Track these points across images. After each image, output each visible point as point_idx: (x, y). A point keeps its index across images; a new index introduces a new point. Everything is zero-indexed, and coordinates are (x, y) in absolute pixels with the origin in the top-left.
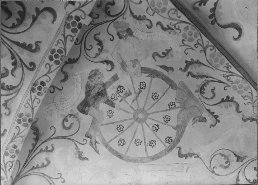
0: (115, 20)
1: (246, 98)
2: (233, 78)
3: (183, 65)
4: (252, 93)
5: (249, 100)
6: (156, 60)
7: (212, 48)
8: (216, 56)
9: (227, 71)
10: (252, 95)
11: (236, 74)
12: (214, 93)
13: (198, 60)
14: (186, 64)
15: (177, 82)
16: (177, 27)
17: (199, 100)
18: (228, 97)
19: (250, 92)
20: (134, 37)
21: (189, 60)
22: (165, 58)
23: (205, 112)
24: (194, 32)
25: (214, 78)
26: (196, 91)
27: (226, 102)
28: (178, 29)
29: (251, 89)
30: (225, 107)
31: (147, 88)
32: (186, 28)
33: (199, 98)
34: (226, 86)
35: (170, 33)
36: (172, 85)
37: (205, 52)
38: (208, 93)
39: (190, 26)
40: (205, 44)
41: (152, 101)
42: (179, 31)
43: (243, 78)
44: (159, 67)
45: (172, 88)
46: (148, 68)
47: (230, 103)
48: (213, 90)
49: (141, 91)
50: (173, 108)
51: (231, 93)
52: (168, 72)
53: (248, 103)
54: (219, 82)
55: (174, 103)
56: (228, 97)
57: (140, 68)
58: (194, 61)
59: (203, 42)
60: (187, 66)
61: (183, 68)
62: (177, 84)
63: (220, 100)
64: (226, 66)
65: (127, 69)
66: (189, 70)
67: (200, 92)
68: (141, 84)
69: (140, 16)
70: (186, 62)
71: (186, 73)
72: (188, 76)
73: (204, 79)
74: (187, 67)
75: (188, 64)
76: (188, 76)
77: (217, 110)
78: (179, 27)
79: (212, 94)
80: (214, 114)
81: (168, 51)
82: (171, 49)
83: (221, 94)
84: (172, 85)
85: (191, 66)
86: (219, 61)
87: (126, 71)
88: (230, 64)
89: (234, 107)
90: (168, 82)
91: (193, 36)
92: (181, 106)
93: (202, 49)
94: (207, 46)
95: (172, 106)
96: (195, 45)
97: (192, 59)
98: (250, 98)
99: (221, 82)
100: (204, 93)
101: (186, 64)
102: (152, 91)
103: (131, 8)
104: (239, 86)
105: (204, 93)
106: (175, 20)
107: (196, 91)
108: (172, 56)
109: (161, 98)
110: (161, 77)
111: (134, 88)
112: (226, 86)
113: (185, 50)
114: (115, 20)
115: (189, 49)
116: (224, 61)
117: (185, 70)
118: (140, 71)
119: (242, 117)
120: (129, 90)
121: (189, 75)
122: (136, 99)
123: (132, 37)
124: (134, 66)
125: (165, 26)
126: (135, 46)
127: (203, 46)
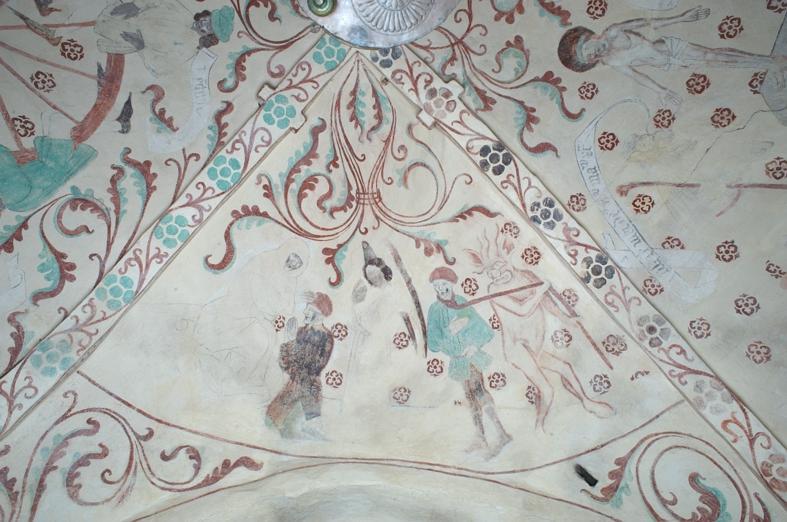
0: (239, 13)
1: (88, 309)
2: (133, 273)
3: (138, 156)
4: (104, 319)
5: (83, 318)
6: (144, 92)
7: (197, 218)
8: (180, 229)
9: (150, 257)
10: (99, 321)
11: (145, 275)
12: (76, 233)
13: (155, 188)
14: (142, 162)
15: (94, 141)
16: (238, 145)
17: (53, 199)
18: (72, 267)
19: (105, 313)
20: (198, 48)
21: (152, 170)
22: (151, 115)
23: (17, 217)
24: (229, 179)
25: (116, 227)
26: (74, 189)
27: (56, 265)
28: (233, 148)
29: (114, 314)
30: (43, 264)
31: (67, 62)
32: (234, 163)
33: (57, 196)
34: (99, 257)
35: (210, 128)
36: (81, 132)
37: (188, 205)
38: (74, 218)
39: (240, 171)
40: (204, 204)
41: (26, 74)
42: (229, 150)
43: (137, 292)
44: (126, 100)
45: (74, 129)
46: (122, 71)
47: (57, 275)
48: (86, 229)
49: (57, 44)
50: (13, 129)
51: (86, 274)
52: (118, 120)
53: (76, 317)
54: (108, 242)
55: (32, 134)
56: (72, 267)
57: (120, 50)
58: (152, 180)
59: (208, 199)
60: (139, 164)
61: (130, 156)
62: (88, 142)
63: (60, 249)
64: (162, 253)
65: (119, 17)
66: (129, 170)
67: (76, 199)
68: (75, 46)
69: (244, 68)
70: (148, 164)
71: (120, 163)
72: (114, 168)
73: (112, 207)
74: (135, 164)
75: (144, 168)
76: (114, 168)
77: (31, 240)
78: (238, 149)
79: (72, 228)
80: (15, 242)
81: (169, 123)
82: (175, 130)
83: (75, 250)
84: (81, 132)
85: (138, 173)
86: (171, 237)
87: (112, 13)
88: (165, 260)
89: (47, 285)
90: (90, 120)
91: (220, 177)
92: (27, 151)
93: (194, 199)
94: (200, 209)
95: (23, 127)
96: (203, 184)
97: (155, 175)
98: (92, 318)
99: (109, 245)
100: (74, 208)
101: (142, 162)
102: (59, 76)
103: (262, 52)
104: (117, 286)
105: (74, 208)
106: (251, 143)
107: (74, 189)
108: (159, 131)
109: (40, 97)
110: (100, 101)
111: (64, 25)
112: (99, 257)
113: (175, 161)
114: (239, 13)
115: (180, 169)
116: (170, 247)
117: (129, 162)
118: (113, 50)
119: (22, 309)
120: (56, 10)
121: (115, 172)
122: (28, 26)
123: (198, 44)
124: (126, 36)
125: (224, 119)
126: (178, 46)
127: (200, 199)
